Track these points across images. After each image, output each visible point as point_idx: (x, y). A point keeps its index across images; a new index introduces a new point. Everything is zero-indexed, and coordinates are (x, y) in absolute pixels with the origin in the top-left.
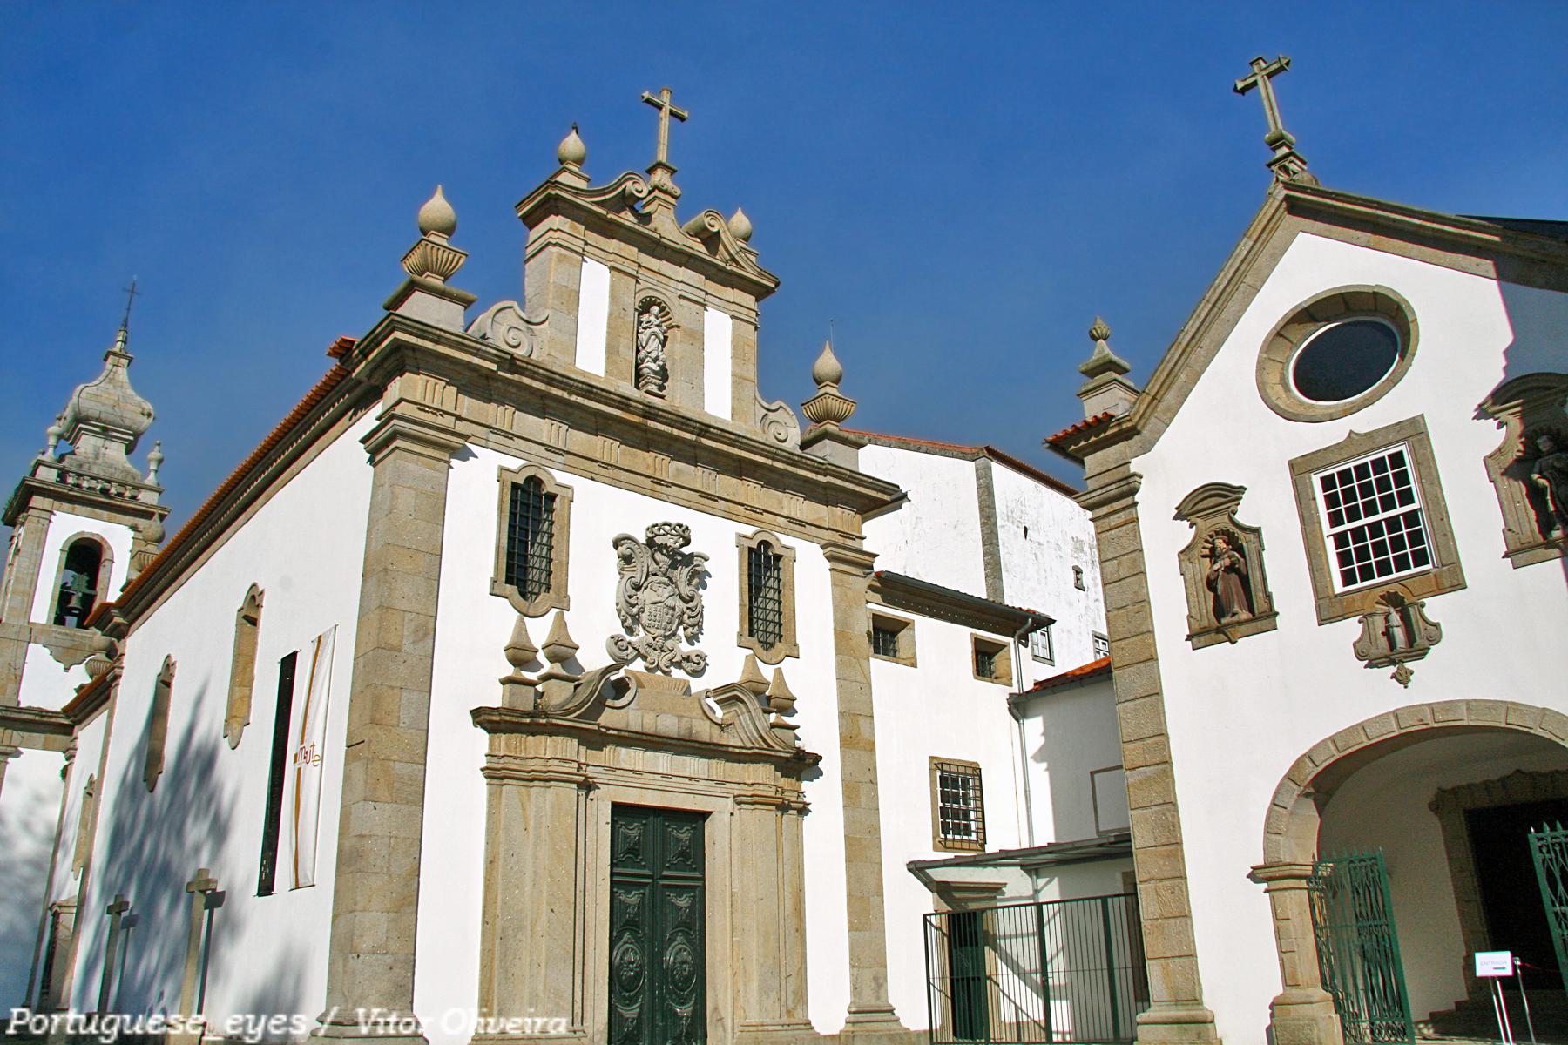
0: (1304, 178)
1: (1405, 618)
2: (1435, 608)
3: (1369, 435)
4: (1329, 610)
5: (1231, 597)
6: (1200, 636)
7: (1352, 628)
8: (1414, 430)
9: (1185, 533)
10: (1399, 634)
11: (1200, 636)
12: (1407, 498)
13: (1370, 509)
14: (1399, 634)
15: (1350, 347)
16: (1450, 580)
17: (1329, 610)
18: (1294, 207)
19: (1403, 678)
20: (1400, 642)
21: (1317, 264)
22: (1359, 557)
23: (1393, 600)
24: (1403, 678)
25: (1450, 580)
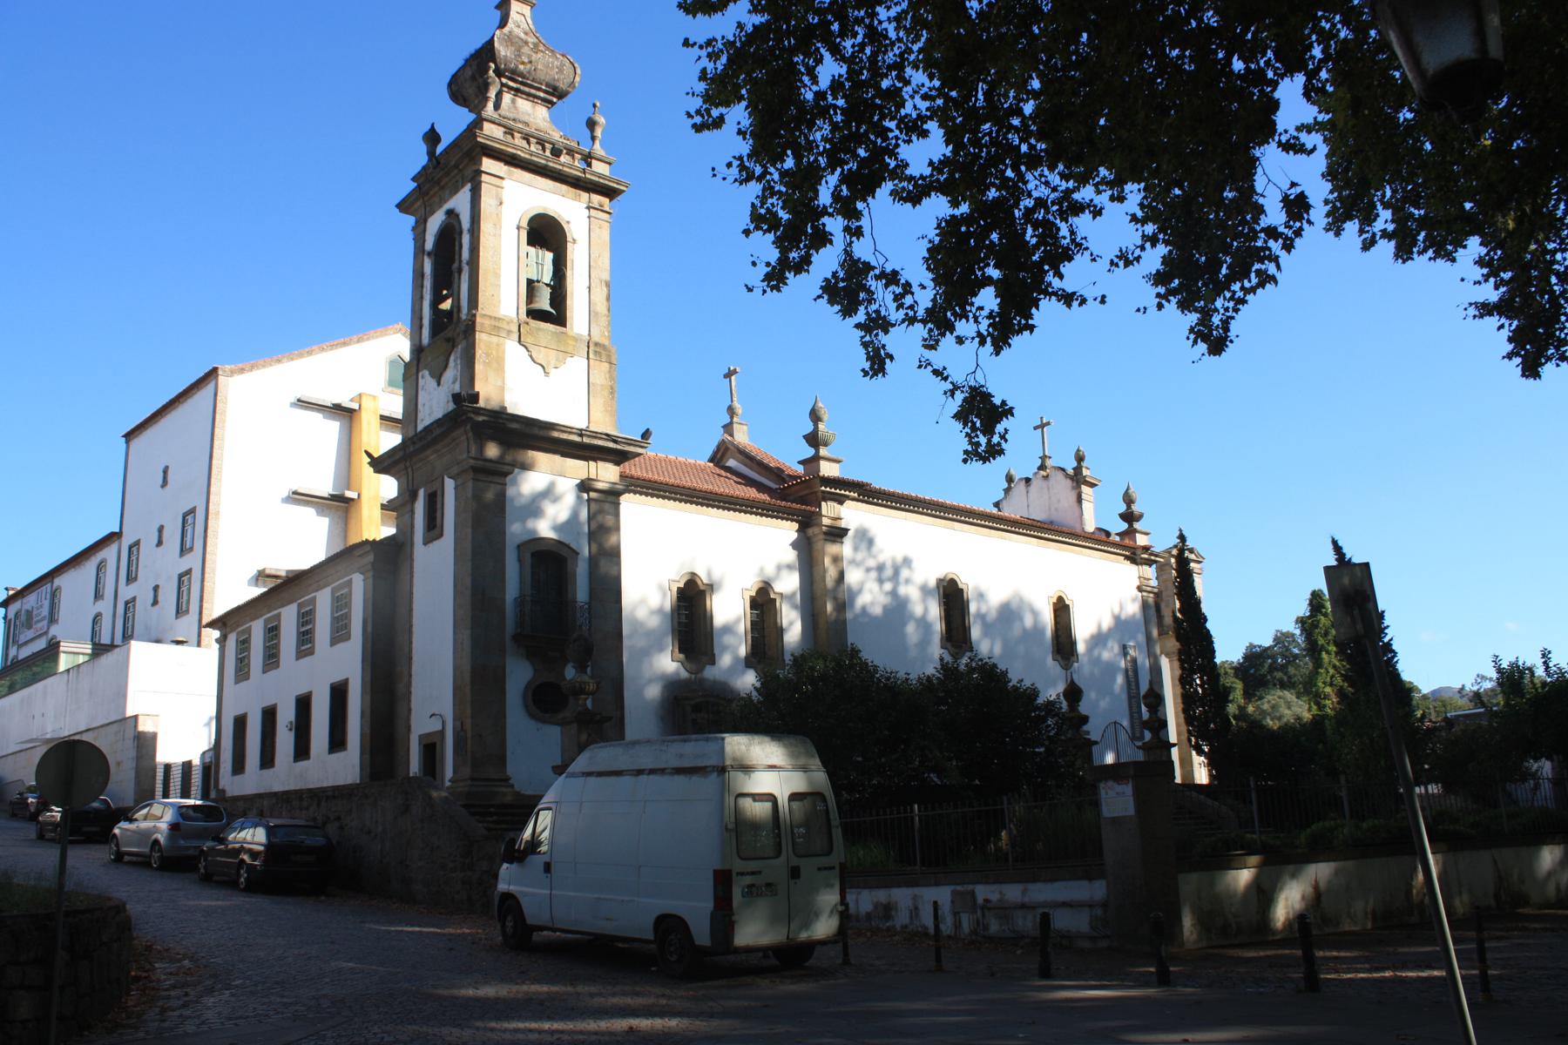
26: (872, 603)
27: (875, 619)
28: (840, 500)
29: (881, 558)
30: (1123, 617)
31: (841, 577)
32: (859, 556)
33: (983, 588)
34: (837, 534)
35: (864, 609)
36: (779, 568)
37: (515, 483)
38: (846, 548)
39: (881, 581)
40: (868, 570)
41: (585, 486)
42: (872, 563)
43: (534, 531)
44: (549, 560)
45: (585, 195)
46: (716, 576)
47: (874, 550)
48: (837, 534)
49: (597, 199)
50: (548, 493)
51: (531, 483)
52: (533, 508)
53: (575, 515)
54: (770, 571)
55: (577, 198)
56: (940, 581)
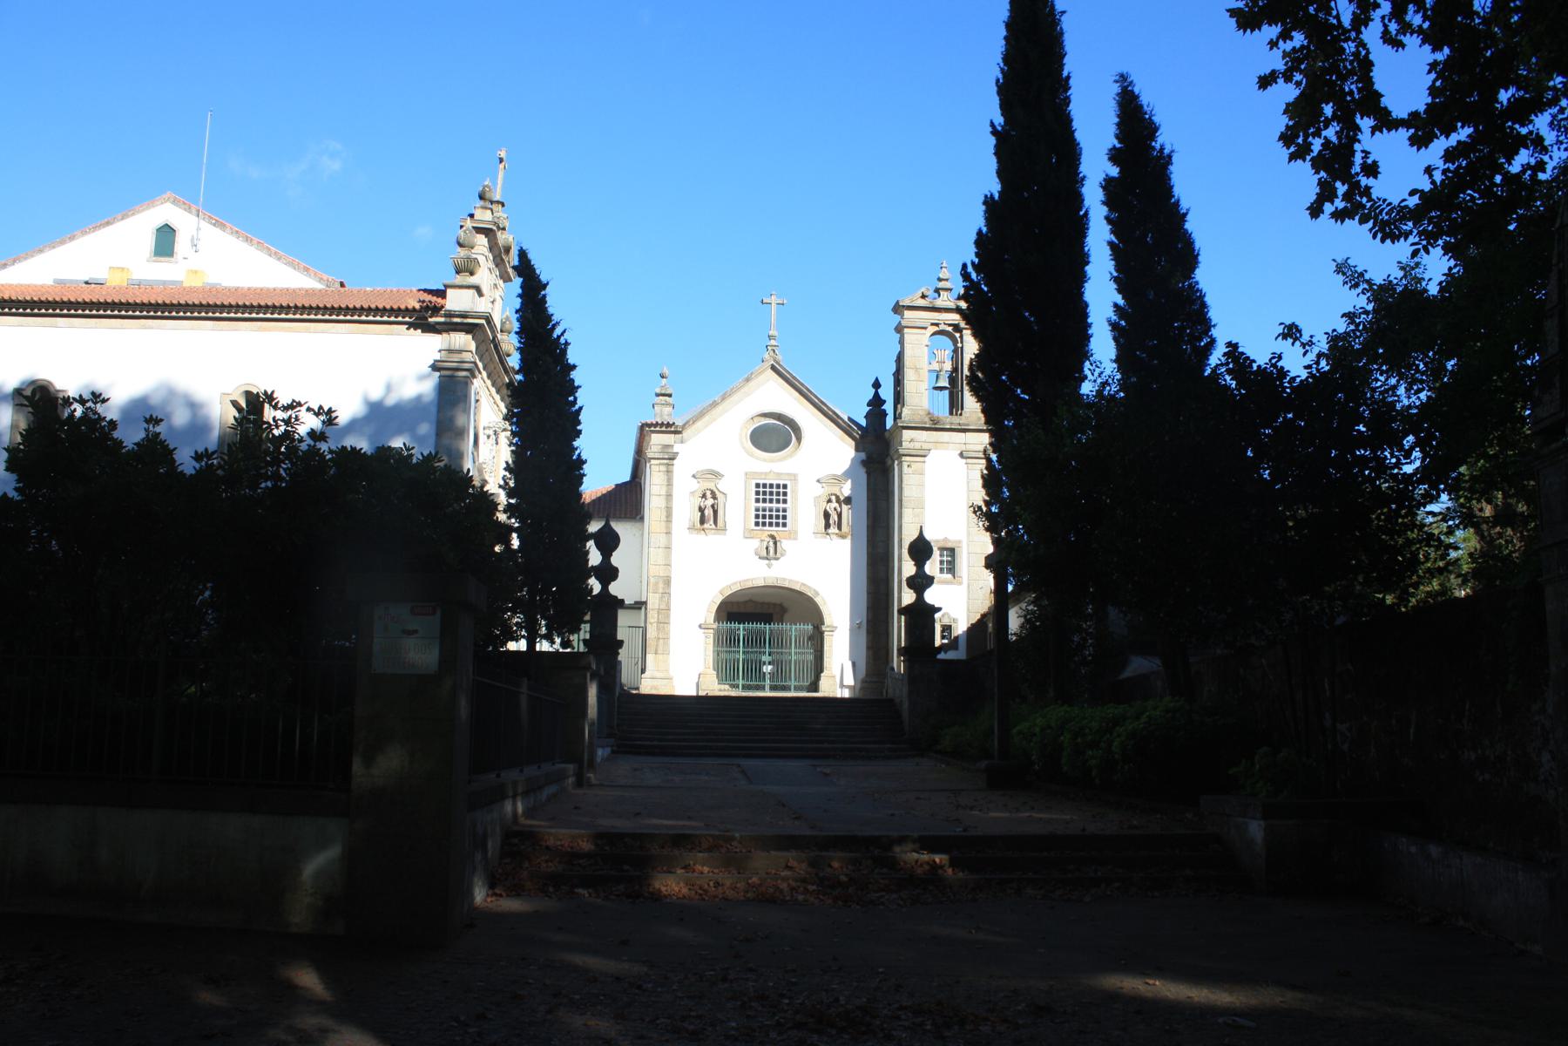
0: (779, 357)
2: (785, 544)
3: (779, 475)
4: (748, 535)
5: (709, 516)
6: (692, 528)
7: (755, 543)
8: (794, 477)
9: (697, 486)
10: (772, 550)
11: (692, 528)
12: (785, 501)
13: (771, 501)
14: (772, 550)
15: (775, 434)
16: (793, 536)
18: (773, 368)
19: (769, 566)
20: (772, 551)
21: (775, 397)
22: (762, 519)
23: (772, 537)
25: (793, 536)
30: (391, 401)
33: (100, 385)
56: (18, 392)
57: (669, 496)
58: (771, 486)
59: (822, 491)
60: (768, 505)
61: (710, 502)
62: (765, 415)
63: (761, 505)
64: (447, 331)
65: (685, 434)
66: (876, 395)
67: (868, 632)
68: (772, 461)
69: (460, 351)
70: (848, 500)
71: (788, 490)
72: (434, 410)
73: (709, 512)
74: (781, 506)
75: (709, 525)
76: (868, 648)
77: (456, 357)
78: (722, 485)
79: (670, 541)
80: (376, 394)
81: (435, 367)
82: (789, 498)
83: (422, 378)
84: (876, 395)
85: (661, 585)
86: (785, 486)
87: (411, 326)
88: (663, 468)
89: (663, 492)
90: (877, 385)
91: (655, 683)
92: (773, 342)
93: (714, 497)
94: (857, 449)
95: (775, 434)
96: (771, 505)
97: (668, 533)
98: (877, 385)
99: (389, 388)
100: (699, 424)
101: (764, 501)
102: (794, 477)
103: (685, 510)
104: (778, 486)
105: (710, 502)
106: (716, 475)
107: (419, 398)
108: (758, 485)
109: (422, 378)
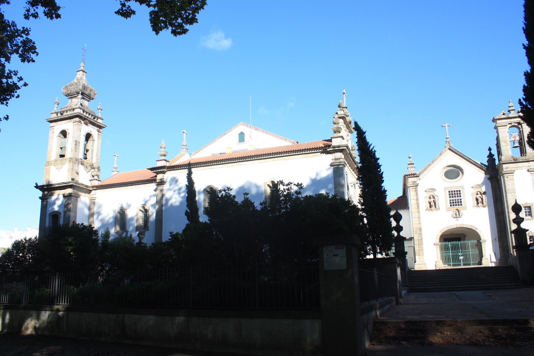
0: (451, 145)
1: (459, 212)
2: (462, 212)
3: (456, 187)
4: (448, 210)
5: (433, 205)
6: (427, 210)
8: (463, 187)
11: (427, 210)
12: (460, 196)
13: (455, 197)
15: (454, 172)
16: (465, 208)
17: (448, 210)
18: (449, 149)
19: (457, 220)
20: (458, 215)
23: (457, 210)
24: (457, 220)
25: (465, 208)
26: (175, 202)
27: (176, 207)
28: (164, 173)
29: (180, 186)
30: (318, 178)
31: (163, 196)
32: (172, 187)
34: (162, 183)
35: (172, 205)
36: (151, 196)
37: (51, 198)
38: (166, 187)
39: (179, 193)
40: (175, 191)
41: (64, 196)
42: (177, 188)
43: (54, 209)
44: (55, 216)
45: (72, 120)
46: (129, 203)
47: (178, 183)
48: (162, 183)
49: (75, 119)
50: (57, 199)
51: (54, 198)
52: (54, 203)
53: (63, 202)
54: (147, 198)
55: (71, 122)
57: (417, 199)
58: (454, 191)
59: (474, 191)
60: (454, 198)
61: (432, 199)
62: (449, 166)
63: (451, 198)
64: (334, 153)
65: (420, 177)
66: (490, 153)
67: (499, 241)
68: (453, 182)
69: (339, 159)
70: (484, 193)
71: (461, 192)
72: (333, 179)
73: (432, 203)
74: (459, 198)
75: (433, 208)
76: (500, 247)
77: (338, 161)
78: (436, 193)
79: (419, 215)
80: (313, 176)
81: (331, 165)
82: (461, 195)
83: (328, 169)
84: (490, 153)
85: (418, 231)
86: (460, 191)
87: (322, 153)
88: (414, 190)
89: (415, 198)
90: (490, 149)
91: (420, 266)
92: (448, 140)
93: (434, 198)
94: (486, 174)
95: (454, 172)
96: (455, 199)
97: (419, 212)
98: (490, 149)
99: (317, 174)
100: (425, 172)
101: (453, 197)
102: (463, 187)
103: (424, 203)
104: (457, 191)
105: (432, 199)
106: (433, 190)
107: (328, 176)
108: (449, 192)
109: (328, 169)
